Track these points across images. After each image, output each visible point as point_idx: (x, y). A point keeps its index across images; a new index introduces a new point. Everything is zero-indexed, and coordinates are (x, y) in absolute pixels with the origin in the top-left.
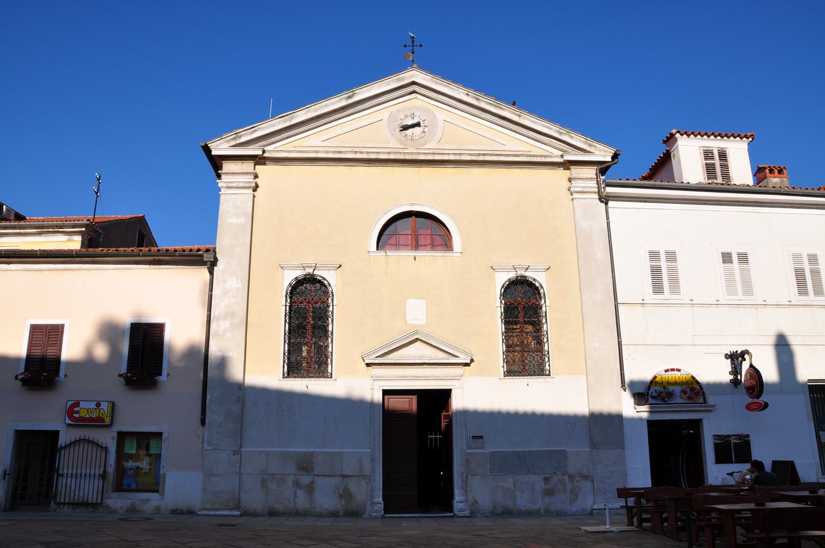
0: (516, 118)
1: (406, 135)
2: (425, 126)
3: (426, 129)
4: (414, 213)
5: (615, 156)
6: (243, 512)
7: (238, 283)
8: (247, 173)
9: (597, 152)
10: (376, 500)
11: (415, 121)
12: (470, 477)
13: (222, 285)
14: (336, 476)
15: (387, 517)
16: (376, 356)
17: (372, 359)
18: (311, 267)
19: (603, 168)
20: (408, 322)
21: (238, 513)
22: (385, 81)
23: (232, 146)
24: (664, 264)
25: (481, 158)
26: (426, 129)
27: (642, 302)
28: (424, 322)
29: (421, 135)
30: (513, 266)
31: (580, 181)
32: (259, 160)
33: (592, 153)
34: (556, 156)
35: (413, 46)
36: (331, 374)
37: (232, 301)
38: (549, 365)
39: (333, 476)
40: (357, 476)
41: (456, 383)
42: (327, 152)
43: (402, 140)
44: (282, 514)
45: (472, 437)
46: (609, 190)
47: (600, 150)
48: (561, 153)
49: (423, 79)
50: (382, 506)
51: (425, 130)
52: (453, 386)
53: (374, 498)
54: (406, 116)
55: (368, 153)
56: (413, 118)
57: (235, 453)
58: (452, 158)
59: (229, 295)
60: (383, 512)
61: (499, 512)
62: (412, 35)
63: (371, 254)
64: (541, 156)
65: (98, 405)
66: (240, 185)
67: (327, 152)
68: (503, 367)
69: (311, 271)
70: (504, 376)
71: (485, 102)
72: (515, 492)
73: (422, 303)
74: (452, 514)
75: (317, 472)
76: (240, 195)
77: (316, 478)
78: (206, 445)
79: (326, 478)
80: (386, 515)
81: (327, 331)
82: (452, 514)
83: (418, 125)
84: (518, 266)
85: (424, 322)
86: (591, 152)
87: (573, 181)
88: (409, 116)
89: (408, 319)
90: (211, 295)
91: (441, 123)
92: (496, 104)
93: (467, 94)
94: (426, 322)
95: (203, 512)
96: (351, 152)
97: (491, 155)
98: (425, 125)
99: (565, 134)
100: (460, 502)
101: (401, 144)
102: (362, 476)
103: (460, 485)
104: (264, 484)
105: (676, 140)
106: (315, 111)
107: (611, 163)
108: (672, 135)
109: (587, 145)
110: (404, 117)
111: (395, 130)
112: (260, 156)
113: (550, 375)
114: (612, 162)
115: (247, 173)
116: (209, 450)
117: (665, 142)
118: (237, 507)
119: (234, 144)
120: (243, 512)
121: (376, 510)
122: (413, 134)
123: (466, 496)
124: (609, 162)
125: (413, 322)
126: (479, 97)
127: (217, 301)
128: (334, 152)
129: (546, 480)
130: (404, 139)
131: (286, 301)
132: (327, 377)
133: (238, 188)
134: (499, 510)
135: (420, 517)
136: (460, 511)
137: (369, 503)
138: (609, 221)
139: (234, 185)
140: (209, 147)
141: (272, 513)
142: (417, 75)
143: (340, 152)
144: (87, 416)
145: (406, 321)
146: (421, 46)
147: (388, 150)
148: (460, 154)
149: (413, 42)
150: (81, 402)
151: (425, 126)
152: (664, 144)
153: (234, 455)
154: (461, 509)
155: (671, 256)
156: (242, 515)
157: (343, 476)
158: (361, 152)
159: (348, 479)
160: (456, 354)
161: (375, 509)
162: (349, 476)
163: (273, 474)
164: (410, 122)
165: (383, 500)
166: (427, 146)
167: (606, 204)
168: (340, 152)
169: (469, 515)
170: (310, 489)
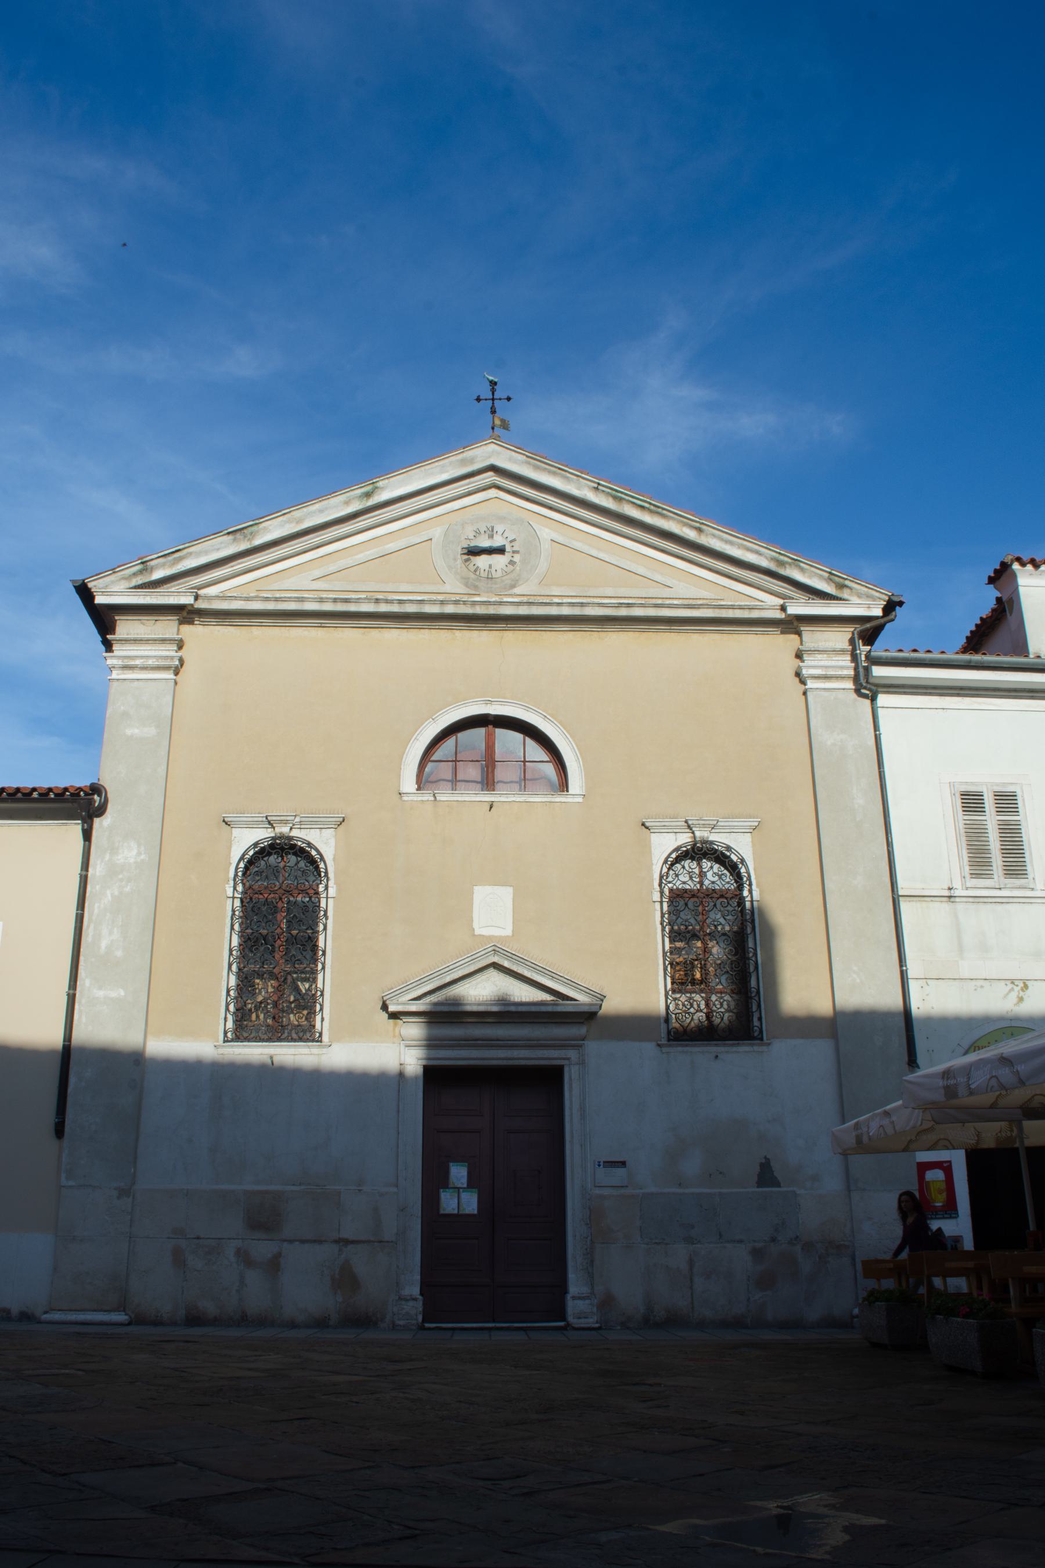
0: (691, 534)
1: (478, 567)
2: (514, 552)
3: (517, 558)
4: (490, 718)
5: (890, 607)
6: (133, 1316)
7: (139, 854)
8: (163, 641)
9: (855, 600)
11: (497, 542)
13: (107, 857)
14: (326, 1241)
15: (430, 1329)
16: (411, 998)
17: (404, 1004)
18: (286, 822)
19: (867, 630)
20: (477, 932)
21: (121, 1317)
22: (437, 464)
23: (135, 587)
24: (991, 819)
25: (623, 612)
26: (517, 558)
27: (946, 893)
28: (508, 932)
29: (505, 568)
30: (686, 822)
31: (819, 657)
32: (186, 614)
33: (844, 600)
34: (772, 608)
35: (493, 399)
36: (321, 1034)
37: (127, 889)
38: (760, 1019)
39: (319, 1242)
40: (369, 1242)
41: (572, 1054)
42: (321, 600)
43: (469, 578)
44: (215, 1322)
45: (604, 1162)
46: (878, 671)
47: (859, 596)
48: (781, 602)
49: (510, 459)
50: (419, 1305)
51: (515, 559)
54: (478, 533)
55: (401, 602)
56: (491, 537)
57: (124, 1193)
58: (566, 611)
59: (121, 876)
60: (420, 1318)
62: (491, 378)
64: (741, 608)
66: (150, 662)
67: (321, 600)
69: (285, 830)
71: (633, 503)
74: (562, 1324)
76: (150, 682)
77: (285, 1244)
78: (63, 1176)
80: (427, 1325)
81: (315, 947)
82: (562, 1324)
83: (501, 551)
85: (508, 932)
86: (841, 599)
87: (805, 657)
88: (483, 532)
89: (475, 925)
90: (86, 877)
91: (546, 545)
92: (652, 507)
93: (597, 489)
94: (513, 931)
95: (52, 1315)
96: (368, 600)
97: (642, 606)
98: (514, 549)
99: (790, 564)
100: (580, 1298)
101: (467, 585)
102: (381, 1242)
104: (178, 1259)
105: (1014, 576)
106: (297, 523)
107: (882, 621)
108: (1005, 567)
109: (833, 585)
110: (474, 534)
111: (455, 560)
112: (190, 608)
113: (762, 1039)
114: (886, 619)
115: (163, 641)
116: (71, 1187)
117: (991, 580)
118: (121, 1307)
119: (140, 582)
120: (133, 1316)
122: (490, 566)
123: (593, 1288)
124: (877, 618)
126: (619, 495)
127: (98, 887)
128: (335, 600)
129: (757, 1254)
130: (472, 576)
131: (235, 888)
132: (313, 1041)
133: (144, 668)
136: (580, 1318)
138: (880, 734)
139: (138, 662)
140: (90, 589)
141: (194, 1319)
142: (499, 453)
143: (346, 601)
145: (474, 930)
146: (509, 399)
147: (441, 597)
148: (582, 605)
149: (493, 391)
151: (514, 552)
152: (992, 586)
153: (119, 1198)
155: (1007, 801)
156: (129, 1324)
158: (387, 601)
159: (350, 1247)
162: (353, 1242)
163: (198, 1238)
164: (485, 543)
165: (421, 1294)
167: (873, 699)
168: (346, 601)
169: (597, 1325)
170: (274, 1266)
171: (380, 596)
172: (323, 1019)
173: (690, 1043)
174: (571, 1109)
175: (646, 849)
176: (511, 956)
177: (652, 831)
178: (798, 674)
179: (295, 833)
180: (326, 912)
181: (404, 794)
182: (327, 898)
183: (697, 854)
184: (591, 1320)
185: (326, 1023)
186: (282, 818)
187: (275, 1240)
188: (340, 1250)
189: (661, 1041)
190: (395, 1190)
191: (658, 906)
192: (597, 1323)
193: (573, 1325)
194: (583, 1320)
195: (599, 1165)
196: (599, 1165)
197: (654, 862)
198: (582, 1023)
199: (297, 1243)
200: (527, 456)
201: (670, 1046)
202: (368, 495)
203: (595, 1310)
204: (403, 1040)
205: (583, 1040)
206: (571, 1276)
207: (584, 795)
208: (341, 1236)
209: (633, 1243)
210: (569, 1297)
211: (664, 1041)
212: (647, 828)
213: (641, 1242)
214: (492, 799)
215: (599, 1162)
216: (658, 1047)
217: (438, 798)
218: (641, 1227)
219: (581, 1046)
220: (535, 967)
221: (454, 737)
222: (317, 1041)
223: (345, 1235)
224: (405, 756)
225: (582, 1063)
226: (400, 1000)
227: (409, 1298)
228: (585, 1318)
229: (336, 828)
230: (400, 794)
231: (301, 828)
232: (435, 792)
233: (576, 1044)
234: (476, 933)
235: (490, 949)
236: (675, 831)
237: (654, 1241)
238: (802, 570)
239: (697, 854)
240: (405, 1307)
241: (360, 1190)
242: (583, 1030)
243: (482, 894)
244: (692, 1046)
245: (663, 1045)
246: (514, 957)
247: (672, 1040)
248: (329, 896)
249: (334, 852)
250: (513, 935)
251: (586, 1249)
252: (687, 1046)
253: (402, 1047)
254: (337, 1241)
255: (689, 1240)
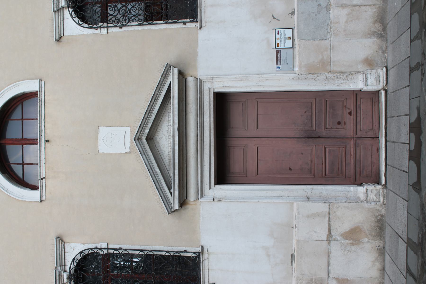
10: (362, 196)
12: (333, 68)
15: (386, 181)
16: (171, 196)
18: (60, 276)
28: (128, 129)
36: (194, 253)
39: (329, 253)
40: (329, 221)
41: (206, 87)
45: (277, 64)
50: (371, 187)
52: (210, 91)
53: (359, 198)
60: (379, 187)
61: (380, 29)
63: (44, 199)
68: (185, 23)
69: (65, 275)
70: (197, 21)
72: (355, 6)
73: (103, 131)
74: (383, 93)
75: (324, 275)
79: (332, 262)
80: (383, 182)
84: (55, 6)
85: (128, 129)
89: (124, 151)
100: (366, 81)
102: (329, 213)
103: (342, 81)
121: (376, 195)
123: (360, 72)
125: (128, 144)
134: (378, 25)
135: (386, 136)
137: (366, 205)
154: (376, 79)
159: (332, 233)
160: (166, 87)
161: (375, 198)
162: (329, 231)
165: (360, 185)
169: (385, 69)
172: (185, 251)
173: (199, 7)
174: (242, 87)
175: (75, 38)
176: (142, 127)
177: (62, 35)
179: (68, 269)
180: (116, 250)
181: (41, 199)
182: (108, 249)
183: (76, 4)
184: (381, 73)
185: (188, 249)
186: (57, 278)
187: (328, 282)
188: (334, 240)
189: (197, 27)
190: (295, 204)
191: (110, 30)
192: (383, 69)
193: (384, 85)
194: (381, 79)
195: (279, 68)
196: (279, 68)
197: (82, 33)
198: (186, 79)
199: (330, 267)
201: (201, 21)
203: (374, 71)
204: (198, 199)
205: (197, 79)
206: (351, 86)
207: (40, 80)
208: (326, 240)
209: (331, 45)
210: (365, 89)
211: (198, 24)
212: (60, 38)
213: (330, 40)
214: (43, 141)
215: (277, 68)
216: (202, 29)
217: (44, 176)
218: (320, 40)
219: (201, 81)
220: (149, 111)
221: (12, 165)
222: (199, 255)
223: (325, 237)
224: (17, 198)
225: (212, 80)
226: (171, 201)
227: (366, 195)
228: (379, 77)
229: (64, 243)
230: (41, 201)
231: (65, 265)
232: (39, 178)
234: (129, 151)
235: (137, 142)
236: (62, 19)
237: (329, 31)
239: (76, 4)
240: (371, 197)
241: (296, 227)
242: (190, 80)
243: (103, 148)
244: (201, 7)
245: (200, 25)
246: (142, 126)
247: (196, 20)
248: (106, 247)
249: (79, 244)
250: (130, 126)
251: (334, 76)
252: (201, 10)
253: (203, 200)
254: (329, 243)
255: (328, 7)
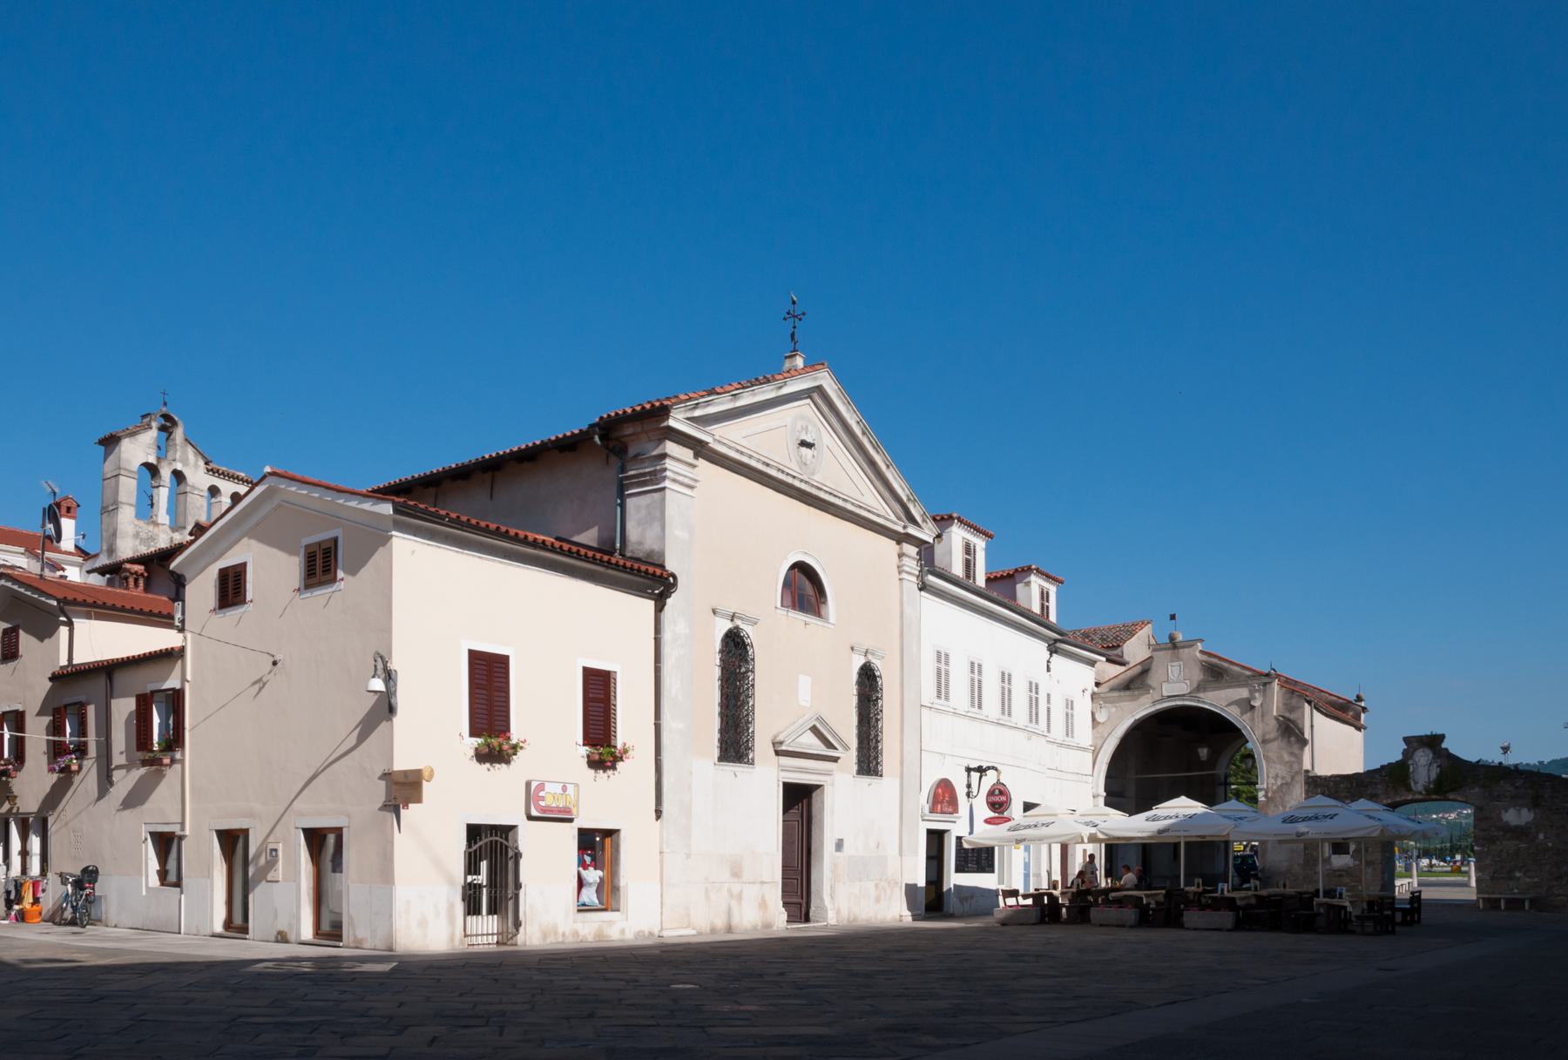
0: (883, 467)
49: (830, 385)
55: (788, 474)
65: (564, 789)
105: (952, 525)
133: (682, 484)
139: (680, 478)
144: (554, 805)
150: (546, 784)
157: (762, 883)
166: (815, 477)
171: (781, 467)
178: (898, 567)
200: (839, 389)
202: (780, 388)
225: (833, 784)
233: (828, 773)
238: (915, 506)
